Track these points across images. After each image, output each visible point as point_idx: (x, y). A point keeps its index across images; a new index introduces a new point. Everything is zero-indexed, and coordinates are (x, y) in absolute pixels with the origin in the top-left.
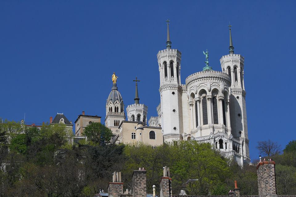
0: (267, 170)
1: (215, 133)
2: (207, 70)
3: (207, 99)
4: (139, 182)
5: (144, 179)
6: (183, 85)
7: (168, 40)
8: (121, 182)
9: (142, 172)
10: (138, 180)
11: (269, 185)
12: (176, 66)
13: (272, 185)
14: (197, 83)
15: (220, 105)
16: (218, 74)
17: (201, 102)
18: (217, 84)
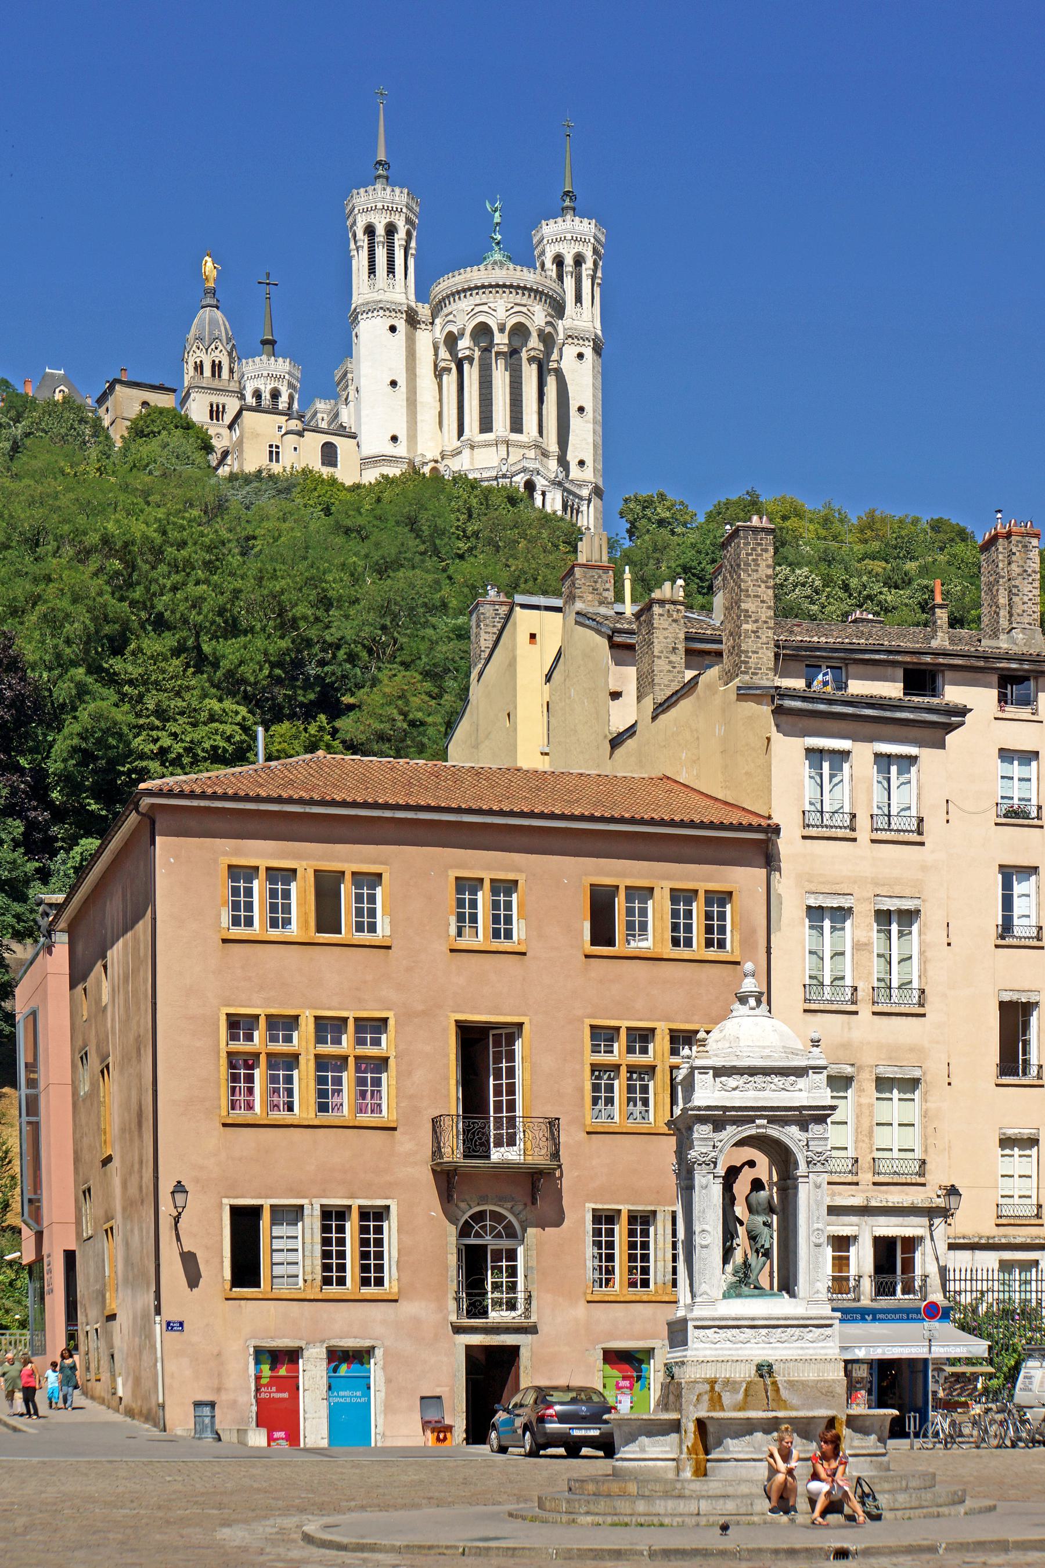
0: (1018, 554)
1: (511, 460)
2: (495, 263)
3: (493, 354)
4: (754, 560)
5: (766, 551)
6: (420, 304)
7: (382, 156)
8: (606, 564)
9: (763, 529)
10: (751, 554)
11: (1022, 599)
12: (404, 243)
13: (1030, 600)
14: (465, 304)
15: (530, 374)
16: (528, 277)
17: (476, 362)
18: (524, 309)
